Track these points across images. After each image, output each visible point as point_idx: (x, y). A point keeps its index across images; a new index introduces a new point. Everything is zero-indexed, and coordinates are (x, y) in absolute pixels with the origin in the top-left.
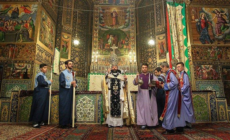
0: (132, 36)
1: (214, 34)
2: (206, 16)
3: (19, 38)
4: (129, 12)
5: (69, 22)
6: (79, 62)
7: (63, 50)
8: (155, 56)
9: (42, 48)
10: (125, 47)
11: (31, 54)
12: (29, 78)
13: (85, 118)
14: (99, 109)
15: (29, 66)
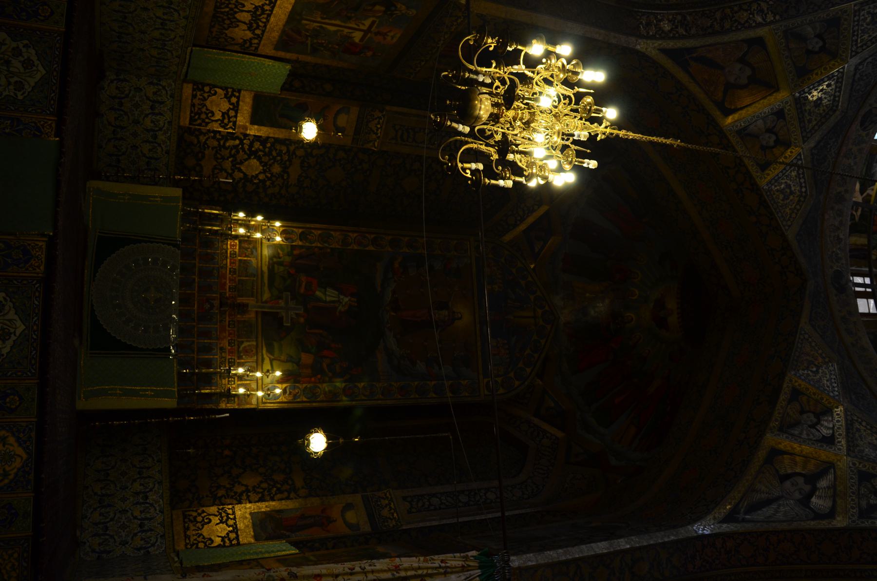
6: (241, 175)
10: (307, 359)
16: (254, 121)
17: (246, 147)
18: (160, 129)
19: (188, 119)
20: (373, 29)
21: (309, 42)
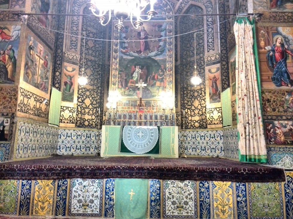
0: (169, 67)
2: (285, 40)
4: (165, 29)
7: (66, 89)
8: (203, 98)
9: (29, 92)
10: (158, 83)
11: (10, 102)
12: (6, 140)
13: (85, 209)
14: (107, 195)
15: (8, 120)
16: (71, 100)
17: (81, 104)
18: (77, 134)
19: (73, 124)
20: (39, 55)
21: (45, 80)
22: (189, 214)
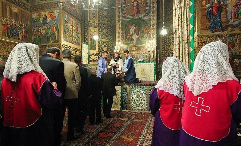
1: (227, 20)
3: (49, 40)
5: (95, 16)
9: (68, 46)
10: (146, 35)
20: (72, 25)
22: (143, 109)
